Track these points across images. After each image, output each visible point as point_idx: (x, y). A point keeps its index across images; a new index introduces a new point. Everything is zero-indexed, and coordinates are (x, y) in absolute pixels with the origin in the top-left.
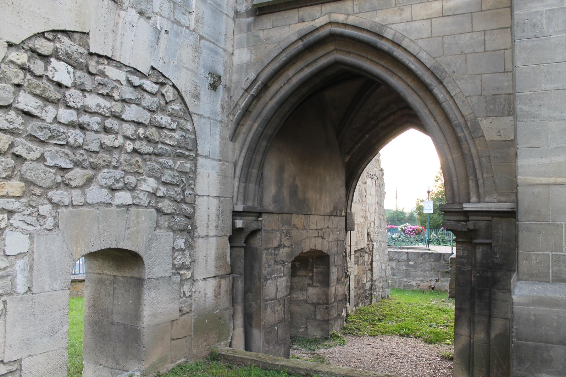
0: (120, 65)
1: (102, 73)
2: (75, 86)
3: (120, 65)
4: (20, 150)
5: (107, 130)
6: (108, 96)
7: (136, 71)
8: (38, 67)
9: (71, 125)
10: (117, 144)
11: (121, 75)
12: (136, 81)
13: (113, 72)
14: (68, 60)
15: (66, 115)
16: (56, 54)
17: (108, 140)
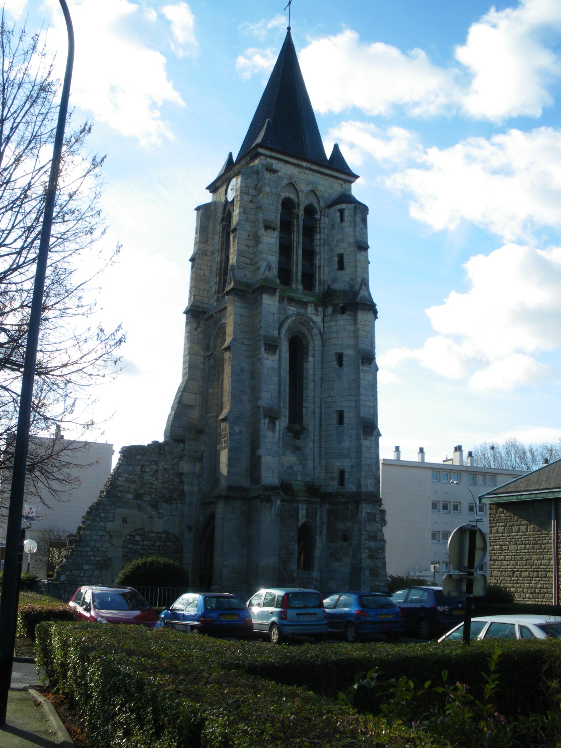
0: (154, 533)
1: (148, 536)
2: (141, 540)
3: (154, 533)
4: (129, 555)
5: (151, 549)
6: (151, 541)
7: (159, 533)
8: (132, 538)
9: (140, 549)
10: (153, 552)
11: (154, 535)
12: (159, 535)
13: (152, 535)
14: (139, 535)
15: (139, 547)
16: (136, 535)
17: (150, 551)
